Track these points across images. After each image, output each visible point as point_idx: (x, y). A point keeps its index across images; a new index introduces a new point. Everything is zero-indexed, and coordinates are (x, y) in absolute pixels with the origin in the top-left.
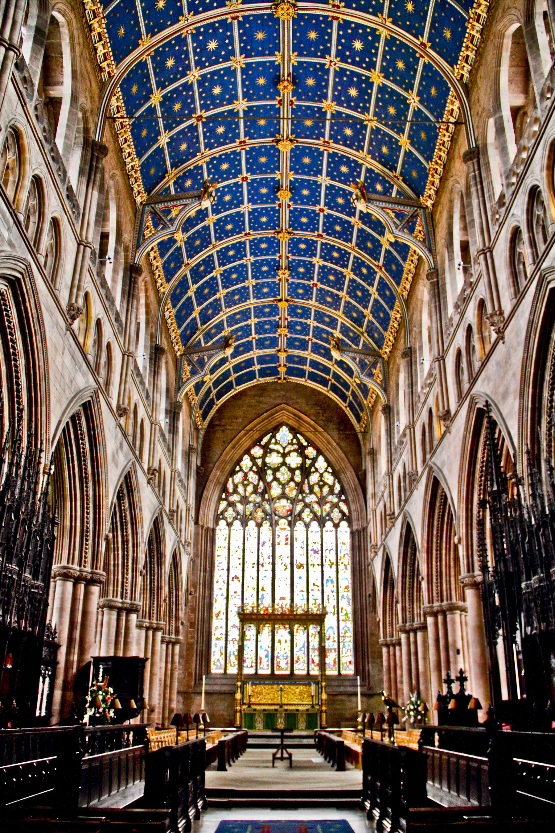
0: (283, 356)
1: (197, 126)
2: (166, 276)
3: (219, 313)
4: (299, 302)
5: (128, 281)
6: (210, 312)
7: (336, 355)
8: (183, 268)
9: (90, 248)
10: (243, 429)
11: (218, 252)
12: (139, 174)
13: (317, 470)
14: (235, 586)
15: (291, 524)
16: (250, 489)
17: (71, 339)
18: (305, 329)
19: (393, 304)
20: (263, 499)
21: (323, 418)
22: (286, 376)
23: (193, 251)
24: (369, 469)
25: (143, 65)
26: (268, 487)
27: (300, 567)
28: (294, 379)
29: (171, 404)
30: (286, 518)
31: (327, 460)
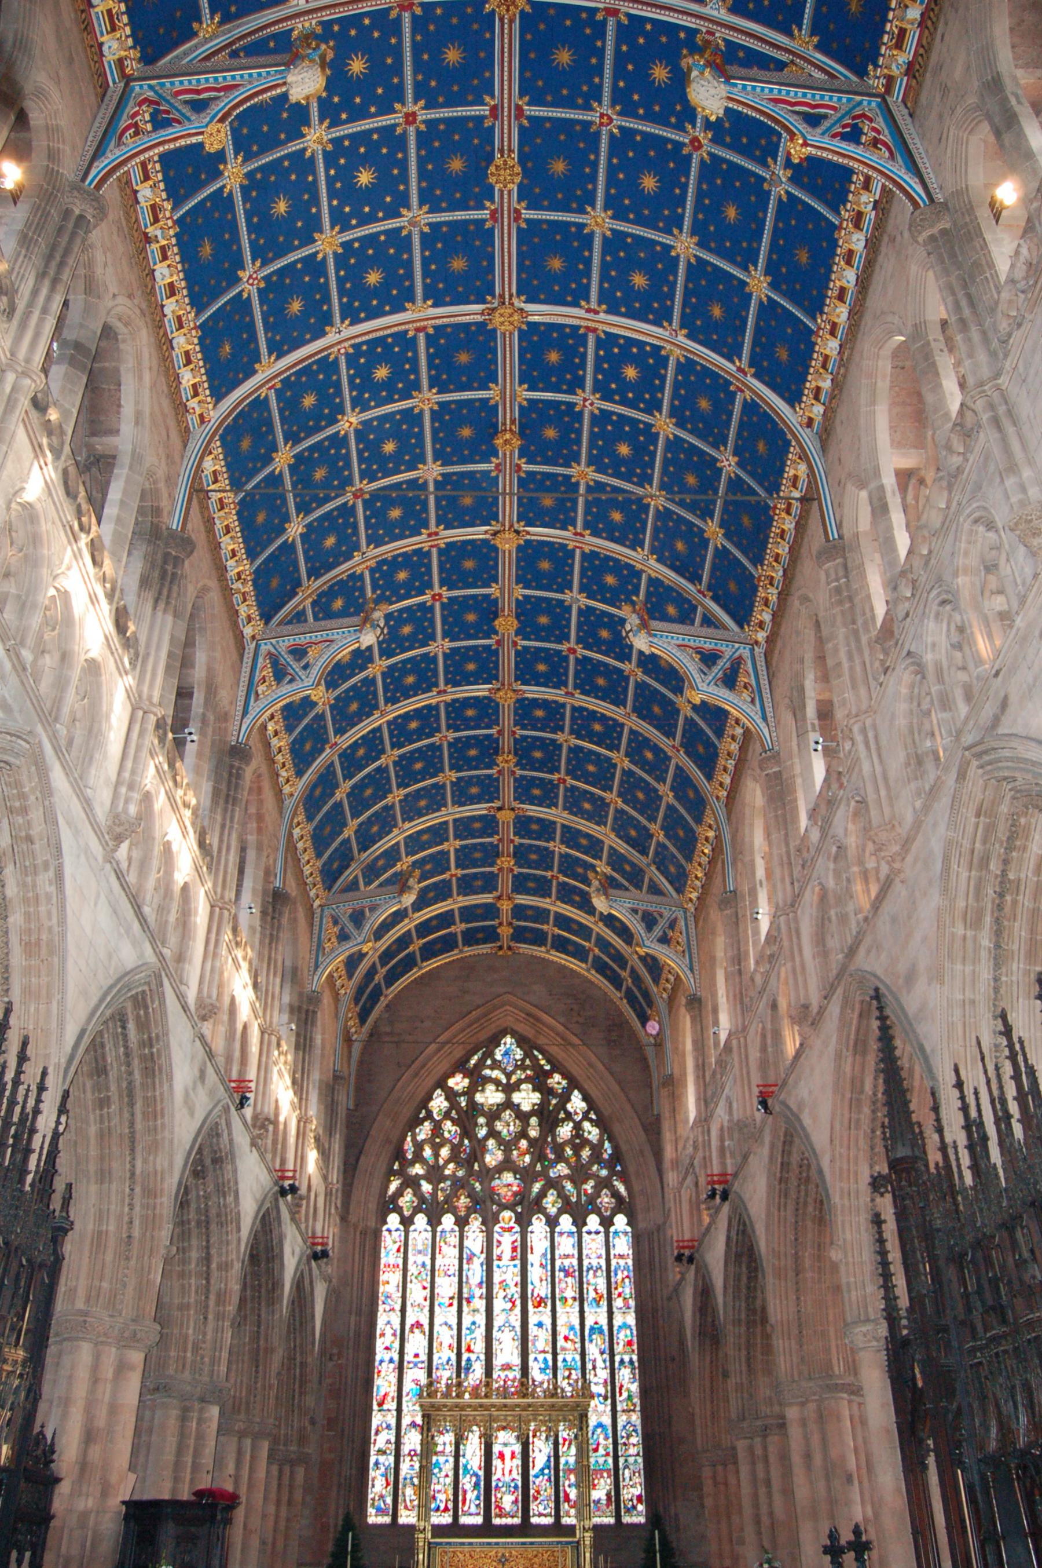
0: (505, 906)
1: (354, 506)
2: (295, 765)
3: (390, 832)
4: (533, 811)
5: (225, 775)
6: (375, 829)
7: (600, 903)
8: (328, 750)
10: (434, 1041)
11: (389, 723)
12: (249, 588)
13: (569, 1116)
14: (416, 1343)
15: (523, 1222)
16: (445, 1152)
17: (113, 878)
18: (545, 859)
19: (702, 813)
20: (470, 1172)
21: (581, 1020)
22: (512, 944)
23: (345, 720)
24: (666, 1114)
25: (259, 404)
26: (479, 1149)
27: (539, 1305)
28: (525, 949)
29: (301, 994)
30: (511, 1207)
31: (585, 1098)
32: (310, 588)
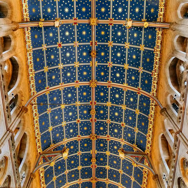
9: (12, 133)
32: (53, 146)
